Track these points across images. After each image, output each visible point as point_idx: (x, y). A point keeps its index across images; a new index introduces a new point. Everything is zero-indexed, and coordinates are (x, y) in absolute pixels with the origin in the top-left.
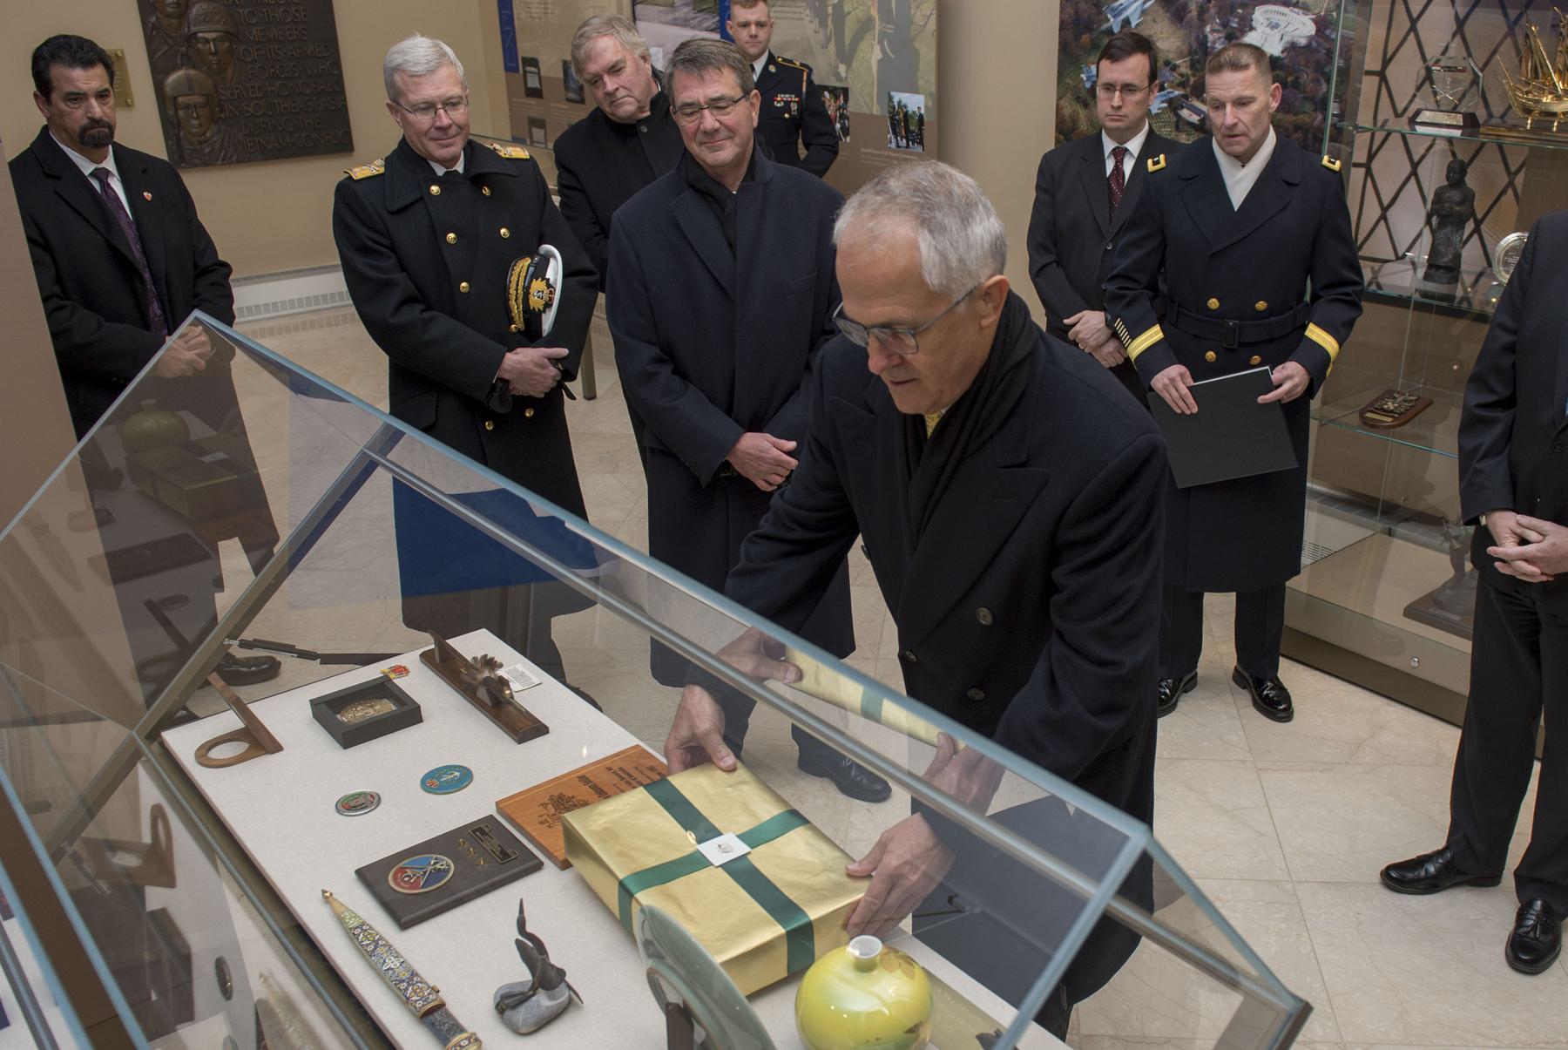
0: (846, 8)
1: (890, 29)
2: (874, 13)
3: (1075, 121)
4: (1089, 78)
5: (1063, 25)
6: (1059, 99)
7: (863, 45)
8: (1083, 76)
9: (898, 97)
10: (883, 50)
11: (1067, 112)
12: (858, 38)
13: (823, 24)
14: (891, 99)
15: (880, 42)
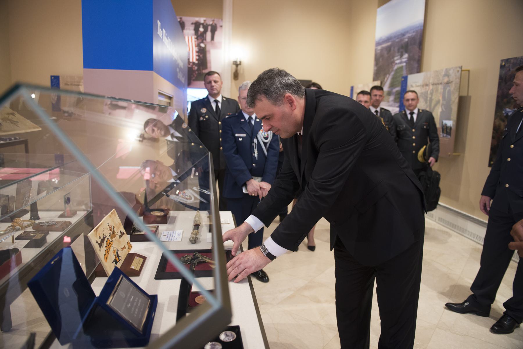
0: (433, 97)
1: (445, 103)
2: (441, 98)
3: (499, 126)
4: (505, 113)
5: (498, 97)
6: (495, 119)
7: (437, 108)
8: (504, 112)
9: (445, 122)
10: (442, 109)
11: (497, 123)
12: (435, 106)
13: (426, 103)
14: (442, 122)
15: (442, 107)
